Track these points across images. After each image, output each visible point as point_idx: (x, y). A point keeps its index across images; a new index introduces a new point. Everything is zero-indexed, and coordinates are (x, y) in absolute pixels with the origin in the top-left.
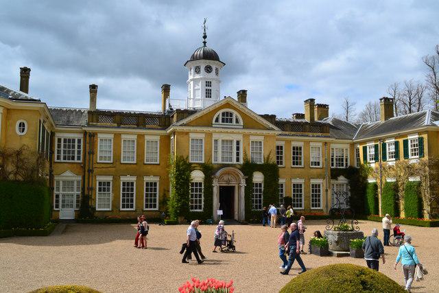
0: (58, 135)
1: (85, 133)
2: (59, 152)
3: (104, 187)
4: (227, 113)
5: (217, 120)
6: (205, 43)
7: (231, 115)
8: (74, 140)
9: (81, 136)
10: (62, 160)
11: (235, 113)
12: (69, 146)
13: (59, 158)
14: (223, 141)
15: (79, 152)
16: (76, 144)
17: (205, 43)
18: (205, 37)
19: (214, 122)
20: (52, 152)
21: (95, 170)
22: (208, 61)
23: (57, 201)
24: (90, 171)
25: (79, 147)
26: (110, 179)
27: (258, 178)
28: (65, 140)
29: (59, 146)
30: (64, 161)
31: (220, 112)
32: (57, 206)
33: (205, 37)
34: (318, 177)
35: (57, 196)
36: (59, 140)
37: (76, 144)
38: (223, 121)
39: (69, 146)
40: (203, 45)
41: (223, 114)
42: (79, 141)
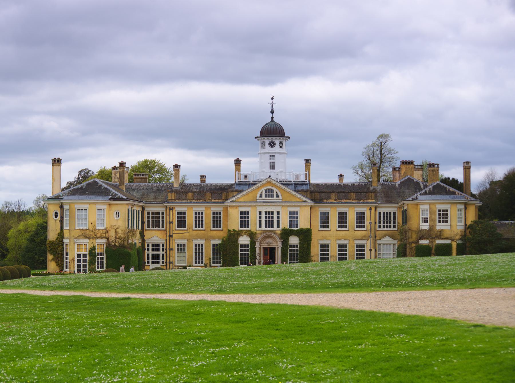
0: (147, 210)
1: (166, 207)
2: (148, 222)
3: (181, 248)
4: (269, 190)
5: (261, 196)
6: (272, 118)
7: (273, 191)
8: (159, 213)
9: (163, 210)
10: (151, 228)
11: (275, 190)
12: (156, 217)
13: (148, 226)
14: (266, 213)
15: (163, 222)
16: (161, 216)
17: (272, 118)
18: (272, 112)
19: (258, 197)
20: (143, 223)
21: (174, 235)
22: (270, 138)
23: (148, 259)
24: (171, 236)
25: (163, 218)
26: (185, 242)
27: (294, 240)
28: (153, 213)
29: (148, 218)
30: (153, 229)
31: (263, 190)
32: (148, 262)
33: (272, 112)
34: (363, 238)
35: (148, 255)
36: (148, 213)
37: (161, 216)
38: (266, 196)
39: (156, 217)
40: (270, 119)
41: (266, 191)
42: (163, 213)
